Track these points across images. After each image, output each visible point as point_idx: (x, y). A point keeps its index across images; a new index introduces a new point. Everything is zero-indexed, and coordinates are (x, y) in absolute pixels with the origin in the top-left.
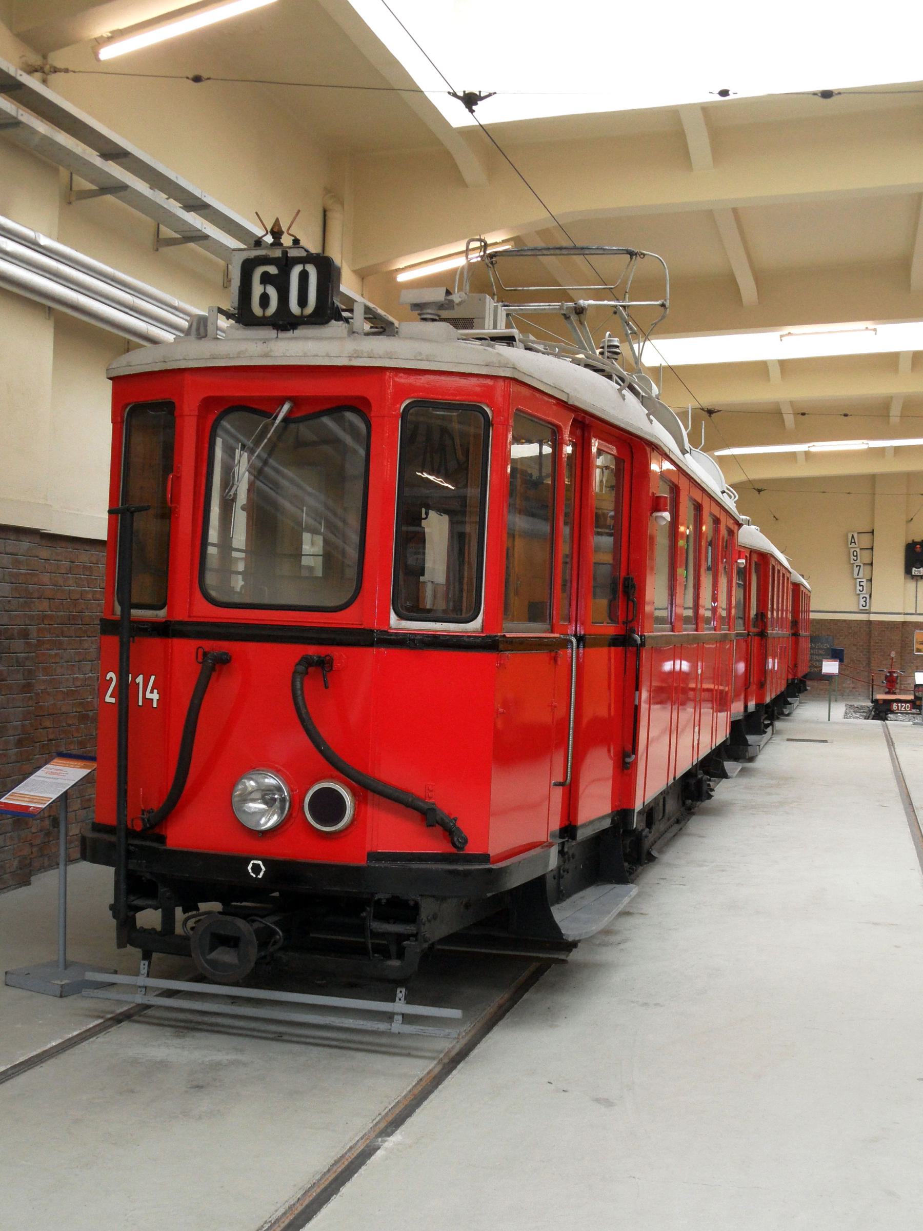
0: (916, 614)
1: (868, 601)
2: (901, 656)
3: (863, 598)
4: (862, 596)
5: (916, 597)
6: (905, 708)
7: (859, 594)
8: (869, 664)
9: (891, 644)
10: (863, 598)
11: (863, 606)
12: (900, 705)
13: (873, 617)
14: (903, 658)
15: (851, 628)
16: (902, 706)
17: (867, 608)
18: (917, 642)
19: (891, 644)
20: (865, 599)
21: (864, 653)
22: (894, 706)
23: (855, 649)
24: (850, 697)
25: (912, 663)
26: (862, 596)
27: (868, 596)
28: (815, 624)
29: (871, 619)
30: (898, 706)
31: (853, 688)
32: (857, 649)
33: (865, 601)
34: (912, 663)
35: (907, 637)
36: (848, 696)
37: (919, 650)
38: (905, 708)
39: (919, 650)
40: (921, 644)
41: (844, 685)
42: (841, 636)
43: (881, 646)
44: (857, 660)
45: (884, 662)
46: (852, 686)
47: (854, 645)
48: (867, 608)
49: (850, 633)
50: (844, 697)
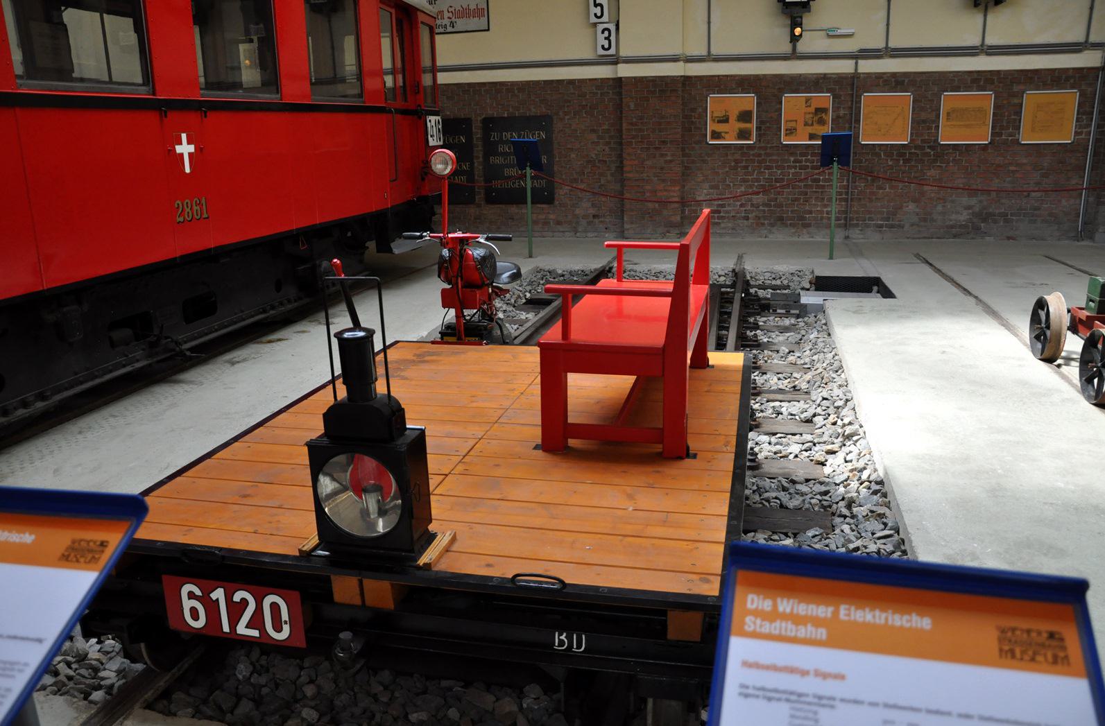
0: (709, 58)
1: (613, 38)
2: (683, 149)
3: (603, 32)
4: (600, 27)
5: (709, 23)
6: (257, 621)
7: (595, 25)
8: (620, 168)
9: (660, 124)
10: (603, 32)
11: (603, 47)
12: (218, 594)
13: (625, 71)
14: (687, 151)
15: (585, 96)
16: (236, 610)
17: (612, 51)
18: (714, 121)
19: (660, 124)
20: (606, 33)
21: (612, 145)
22: (187, 604)
23: (594, 137)
24: (590, 235)
25: (704, 161)
26: (600, 27)
27: (612, 27)
28: (516, 91)
29: (620, 75)
30: (211, 608)
31: (594, 216)
32: (600, 137)
33: (608, 38)
34: (704, 161)
35: (693, 110)
36: (585, 231)
37: (716, 135)
38: (257, 621)
39: (716, 135)
40: (719, 122)
41: (577, 211)
42: (566, 113)
43: (641, 130)
44: (600, 161)
45: (649, 163)
46: (592, 211)
47: (593, 131)
48: (612, 51)
49: (584, 107)
50: (578, 234)
